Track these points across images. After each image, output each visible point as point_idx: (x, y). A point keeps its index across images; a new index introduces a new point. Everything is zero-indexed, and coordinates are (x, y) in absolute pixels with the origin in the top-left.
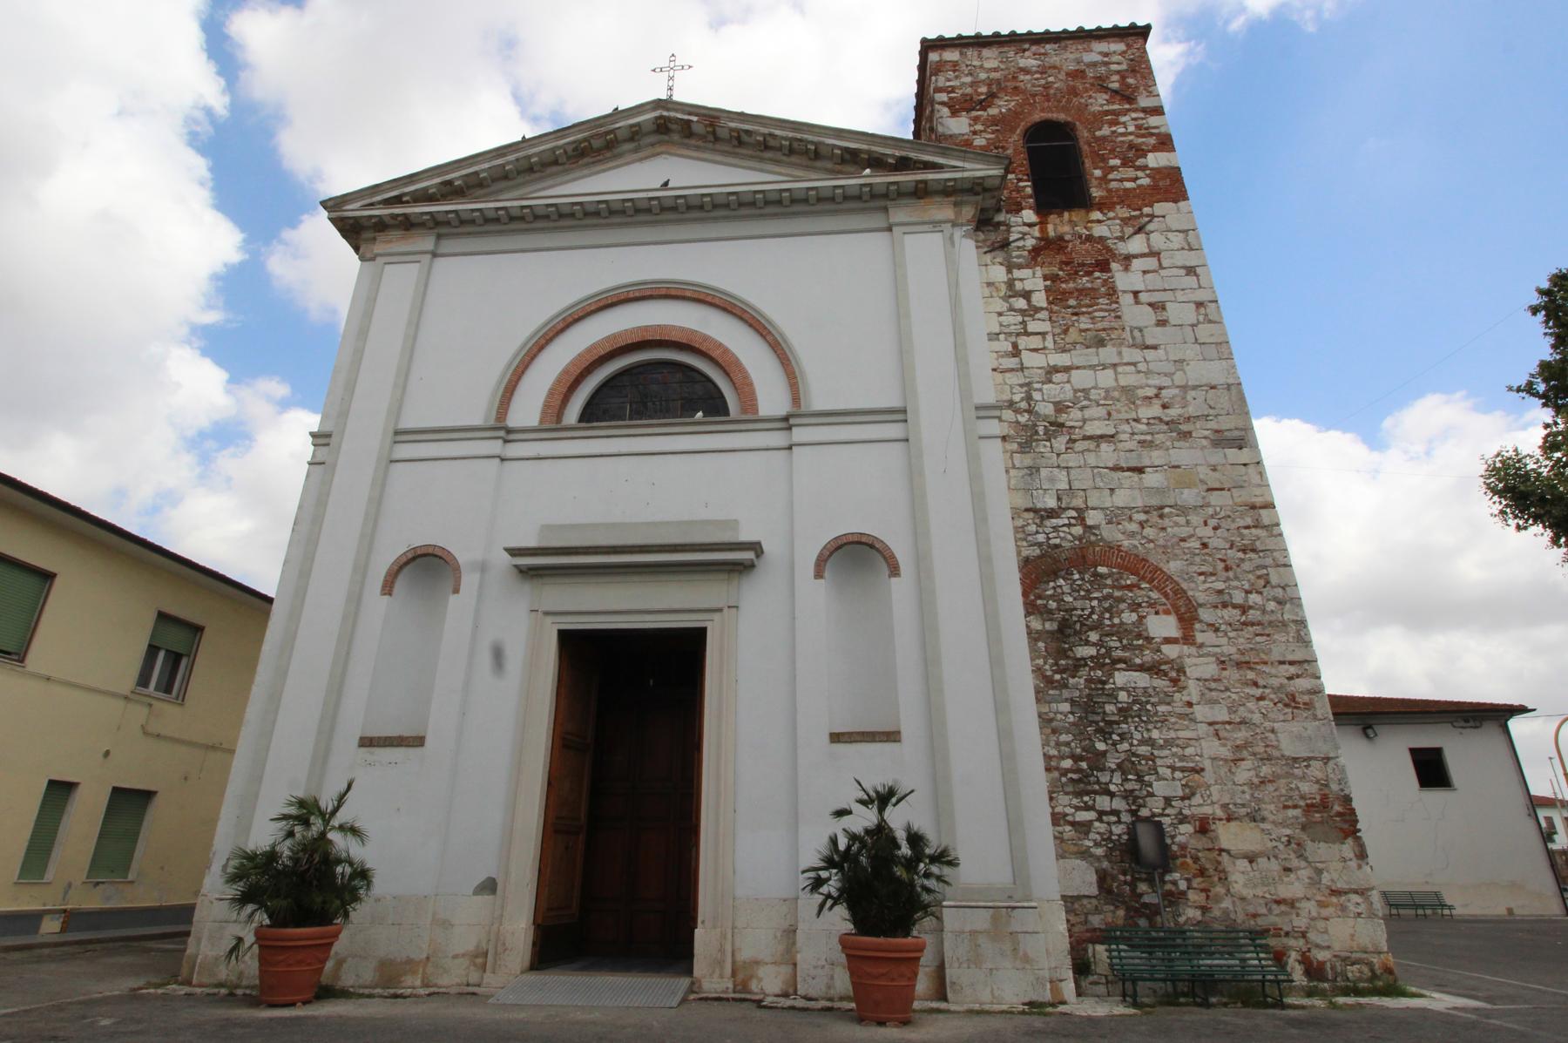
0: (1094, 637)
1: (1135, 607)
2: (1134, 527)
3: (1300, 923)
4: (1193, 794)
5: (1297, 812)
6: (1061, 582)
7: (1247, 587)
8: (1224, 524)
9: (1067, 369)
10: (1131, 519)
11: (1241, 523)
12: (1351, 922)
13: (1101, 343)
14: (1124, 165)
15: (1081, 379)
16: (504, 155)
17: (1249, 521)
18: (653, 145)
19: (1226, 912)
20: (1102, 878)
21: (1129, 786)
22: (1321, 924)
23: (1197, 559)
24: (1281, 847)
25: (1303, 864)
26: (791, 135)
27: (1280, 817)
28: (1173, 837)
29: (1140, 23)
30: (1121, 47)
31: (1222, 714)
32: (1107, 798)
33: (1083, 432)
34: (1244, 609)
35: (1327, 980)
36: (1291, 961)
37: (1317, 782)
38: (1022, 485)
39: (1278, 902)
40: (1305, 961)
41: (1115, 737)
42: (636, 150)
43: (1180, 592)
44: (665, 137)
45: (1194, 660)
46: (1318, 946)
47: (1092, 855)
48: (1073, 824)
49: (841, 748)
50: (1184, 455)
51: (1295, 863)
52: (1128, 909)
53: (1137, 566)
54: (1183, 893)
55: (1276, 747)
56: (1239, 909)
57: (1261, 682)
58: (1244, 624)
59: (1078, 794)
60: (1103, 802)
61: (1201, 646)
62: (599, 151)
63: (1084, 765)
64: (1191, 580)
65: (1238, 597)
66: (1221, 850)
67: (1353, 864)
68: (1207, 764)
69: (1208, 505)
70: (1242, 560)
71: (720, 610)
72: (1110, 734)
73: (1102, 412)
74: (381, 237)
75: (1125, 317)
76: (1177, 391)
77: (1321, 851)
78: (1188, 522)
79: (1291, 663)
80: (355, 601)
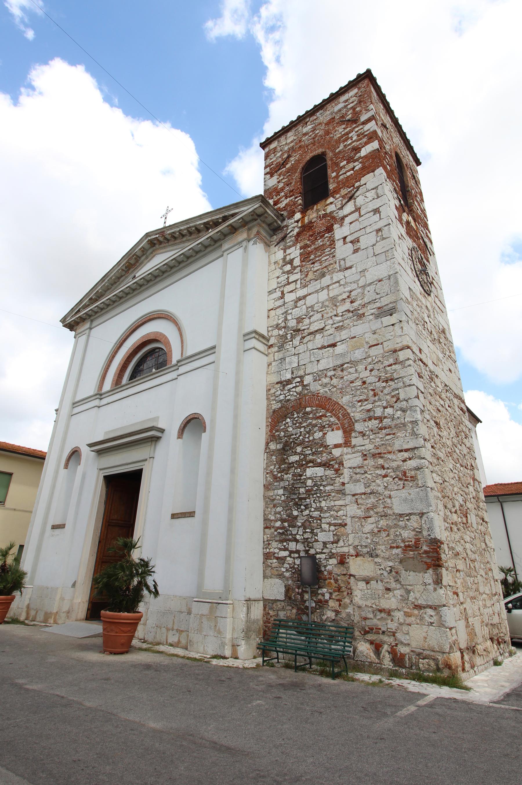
0: (299, 449)
1: (322, 428)
2: (327, 380)
3: (392, 626)
4: (339, 540)
5: (398, 551)
6: (288, 420)
7: (385, 405)
8: (376, 367)
9: (304, 297)
10: (326, 376)
11: (387, 363)
12: (425, 628)
13: (323, 275)
14: (348, 163)
15: (310, 300)
16: (104, 280)
17: (391, 361)
18: (152, 253)
19: (349, 615)
20: (288, 590)
21: (306, 536)
22: (405, 628)
23: (358, 392)
24: (386, 574)
25: (398, 586)
26: (186, 227)
27: (387, 554)
28: (325, 566)
29: (362, 71)
30: (356, 91)
31: (360, 488)
32: (294, 543)
33: (309, 331)
34: (381, 419)
35: (405, 667)
36: (384, 650)
37: (414, 530)
38: (277, 370)
39: (381, 611)
40: (393, 652)
41: (303, 507)
42: (147, 258)
43: (346, 415)
44: (154, 248)
45: (349, 456)
46: (402, 643)
47: (284, 577)
48: (277, 558)
49: (174, 521)
50: (359, 329)
51: (393, 585)
52: (298, 609)
53: (326, 404)
54: (327, 601)
55: (390, 508)
56: (356, 614)
57: (386, 466)
58: (381, 429)
59: (281, 541)
60: (292, 546)
61: (354, 446)
62: (134, 265)
63: (286, 524)
64: (354, 406)
65: (378, 412)
66: (351, 575)
67: (431, 588)
68: (348, 521)
69: (369, 356)
70: (384, 387)
71: (146, 460)
72: (301, 505)
73: (319, 316)
74: (78, 327)
75: (337, 256)
76: (359, 290)
77: (411, 578)
78: (356, 370)
79: (406, 450)
80: (57, 472)
